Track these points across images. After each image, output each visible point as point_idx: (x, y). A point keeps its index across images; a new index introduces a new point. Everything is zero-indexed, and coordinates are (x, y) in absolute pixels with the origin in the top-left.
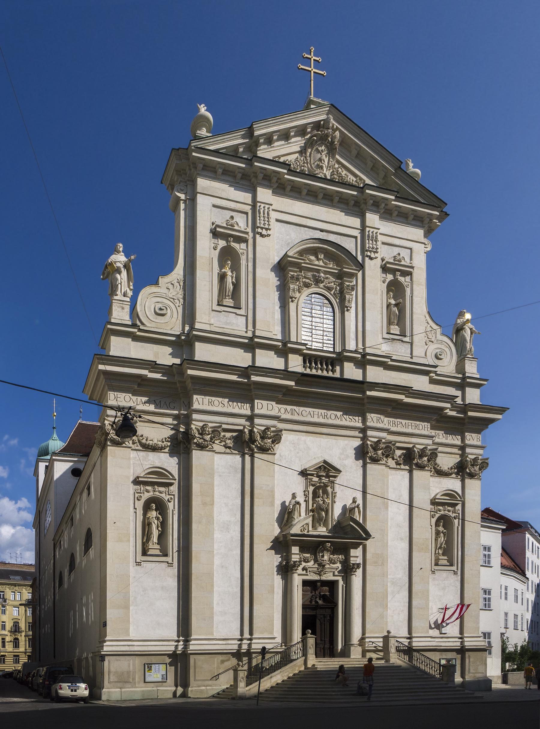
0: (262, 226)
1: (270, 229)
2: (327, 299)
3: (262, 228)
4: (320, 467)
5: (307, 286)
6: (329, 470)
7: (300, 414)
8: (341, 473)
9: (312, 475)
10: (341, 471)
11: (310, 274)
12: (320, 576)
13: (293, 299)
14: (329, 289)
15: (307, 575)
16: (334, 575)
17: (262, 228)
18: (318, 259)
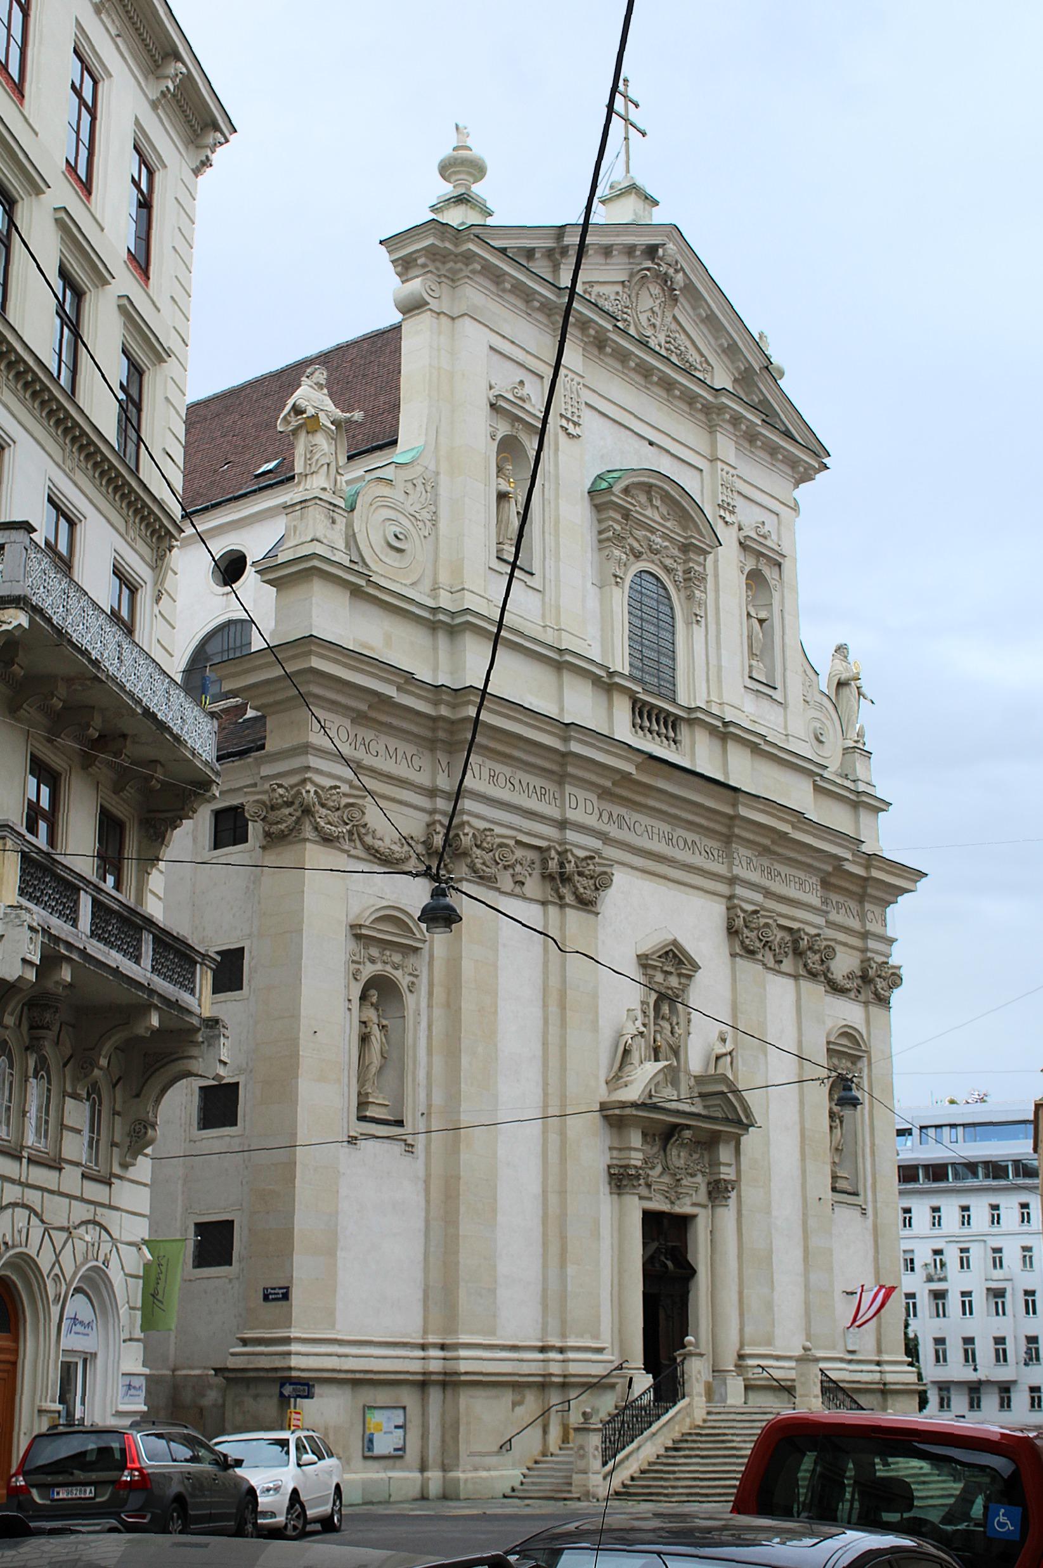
0: (569, 416)
1: (579, 425)
2: (665, 589)
3: (568, 420)
4: (667, 953)
5: (638, 556)
6: (681, 962)
7: (632, 829)
8: (700, 971)
9: (654, 967)
10: (700, 968)
11: (641, 533)
12: (672, 1203)
13: (618, 580)
14: (668, 570)
15: (650, 1199)
16: (694, 1205)
17: (568, 420)
18: (652, 505)
